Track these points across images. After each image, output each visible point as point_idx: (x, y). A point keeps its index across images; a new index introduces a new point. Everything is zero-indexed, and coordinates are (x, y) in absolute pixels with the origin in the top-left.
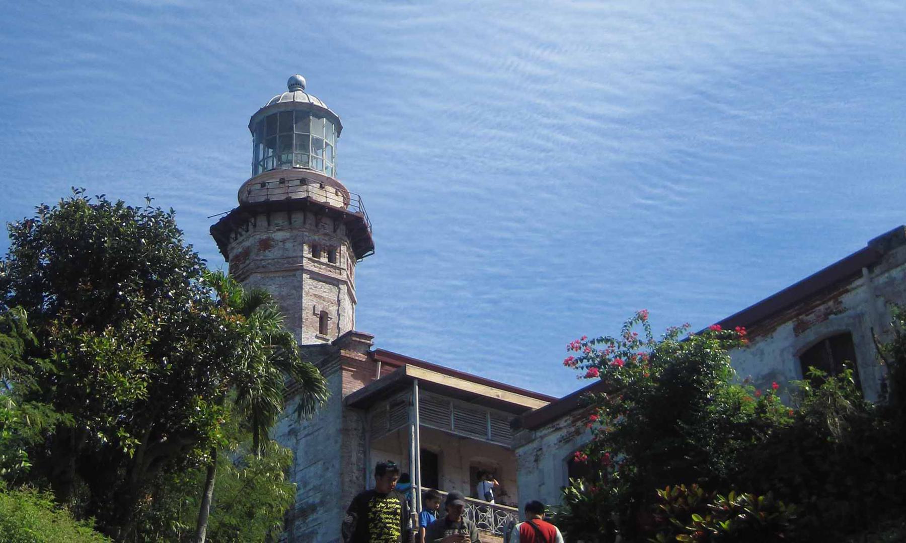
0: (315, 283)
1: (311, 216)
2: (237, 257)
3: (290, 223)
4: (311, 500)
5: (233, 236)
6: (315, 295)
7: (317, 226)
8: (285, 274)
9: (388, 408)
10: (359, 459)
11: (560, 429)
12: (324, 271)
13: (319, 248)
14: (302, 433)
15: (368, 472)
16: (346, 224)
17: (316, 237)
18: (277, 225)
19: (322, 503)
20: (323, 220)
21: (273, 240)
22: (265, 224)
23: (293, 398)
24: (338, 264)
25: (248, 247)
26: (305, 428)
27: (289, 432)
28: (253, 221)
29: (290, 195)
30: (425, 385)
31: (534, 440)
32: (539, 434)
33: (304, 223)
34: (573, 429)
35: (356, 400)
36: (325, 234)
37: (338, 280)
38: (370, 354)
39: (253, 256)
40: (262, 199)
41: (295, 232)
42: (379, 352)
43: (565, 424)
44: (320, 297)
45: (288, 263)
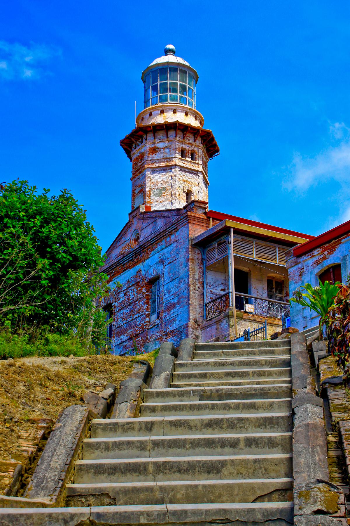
0: (183, 173)
1: (179, 132)
3: (167, 137)
4: (172, 302)
5: (134, 146)
6: (184, 181)
7: (184, 138)
8: (165, 168)
9: (216, 245)
10: (200, 276)
12: (189, 166)
13: (185, 152)
14: (166, 262)
15: (205, 284)
16: (201, 137)
17: (184, 146)
19: (178, 303)
20: (187, 135)
21: (158, 148)
22: (152, 138)
23: (161, 241)
24: (197, 162)
26: (168, 259)
27: (159, 262)
28: (145, 137)
29: (166, 120)
30: (237, 232)
32: (302, 259)
33: (176, 136)
34: (322, 256)
35: (197, 241)
36: (189, 144)
37: (197, 171)
38: (205, 213)
41: (170, 144)
43: (317, 253)
44: (187, 181)
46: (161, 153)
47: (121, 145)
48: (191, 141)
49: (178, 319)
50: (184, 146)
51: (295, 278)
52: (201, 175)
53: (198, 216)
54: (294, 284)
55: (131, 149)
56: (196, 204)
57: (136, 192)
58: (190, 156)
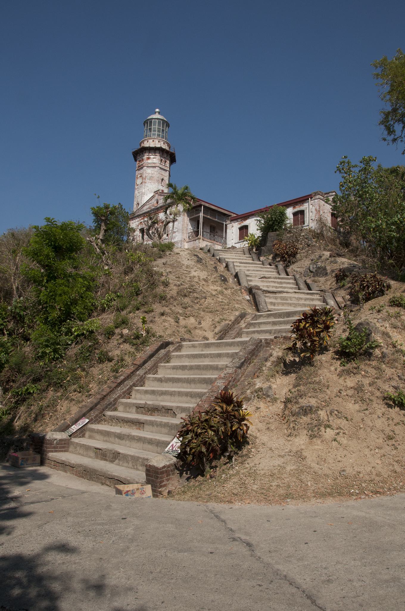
0: (160, 170)
30: (205, 207)
39: (144, 161)
40: (148, 146)
49: (177, 237)
57: (138, 176)
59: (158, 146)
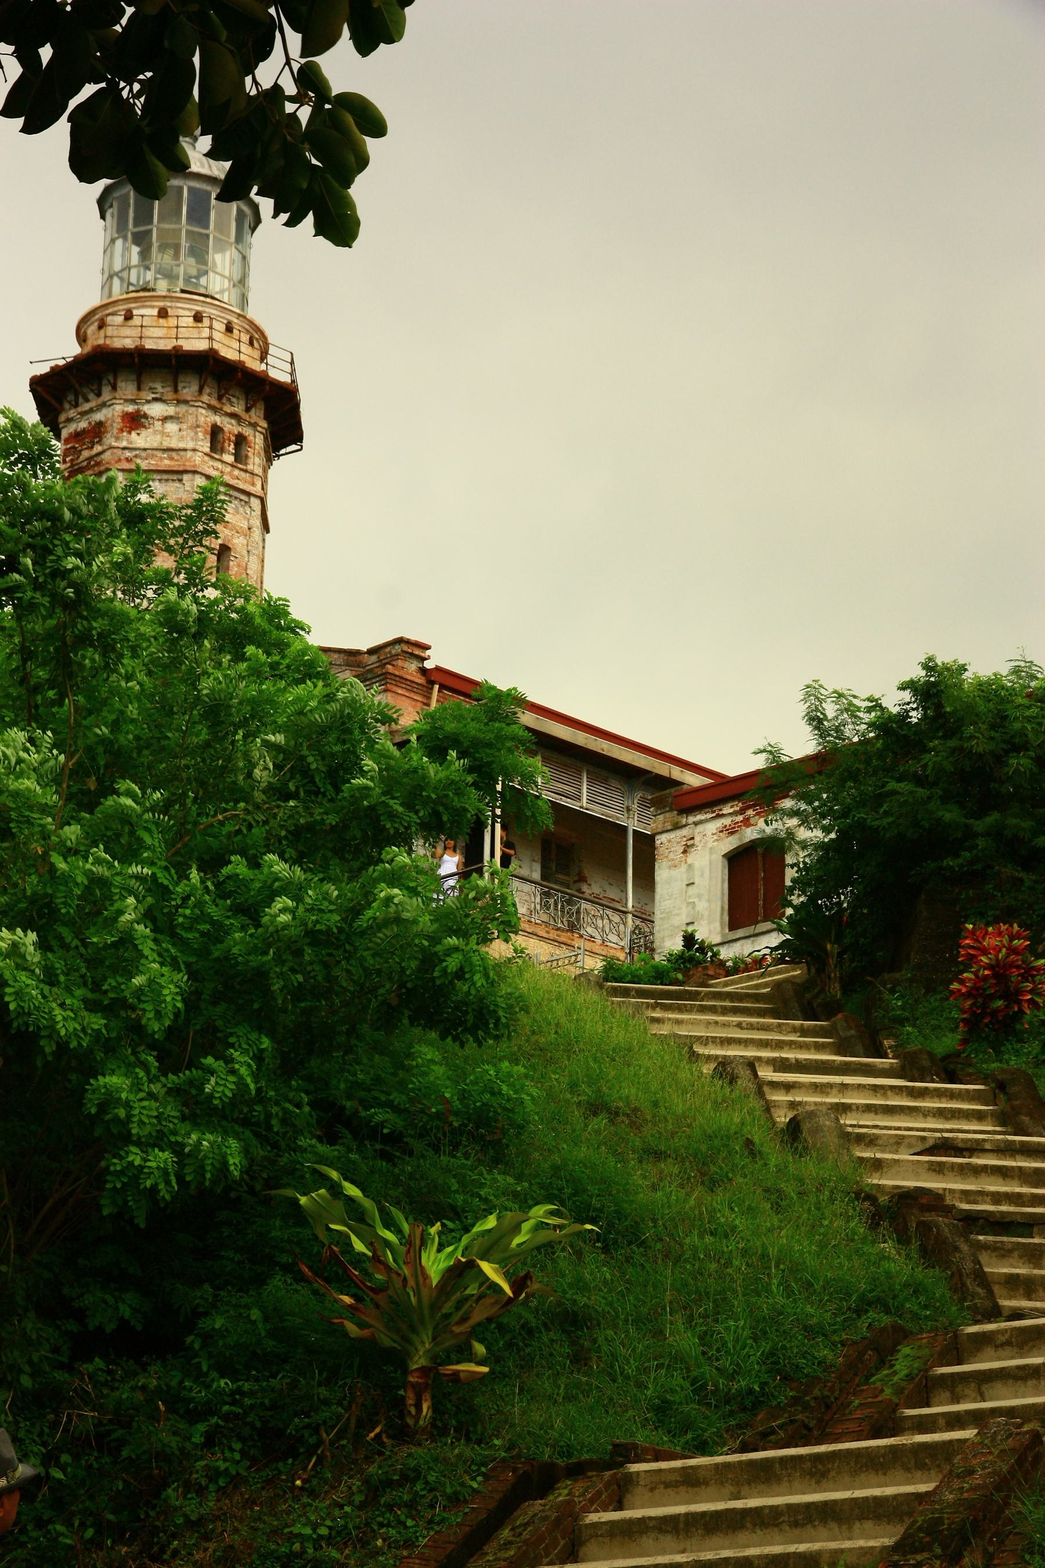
2: (77, 436)
3: (176, 391)
5: (71, 397)
7: (220, 398)
8: (165, 477)
11: (723, 815)
17: (218, 419)
18: (152, 390)
21: (146, 416)
24: (250, 467)
25: (100, 424)
29: (180, 342)
31: (685, 826)
32: (691, 819)
36: (233, 415)
37: (249, 494)
38: (423, 671)
39: (109, 440)
40: (129, 344)
41: (183, 409)
42: (438, 669)
43: (731, 811)
45: (171, 459)
46: (155, 432)
47: (33, 390)
48: (238, 408)
50: (218, 419)
51: (671, 856)
52: (255, 503)
53: (409, 677)
54: (670, 867)
55: (61, 404)
56: (405, 648)
58: (231, 448)
59: (195, 343)
